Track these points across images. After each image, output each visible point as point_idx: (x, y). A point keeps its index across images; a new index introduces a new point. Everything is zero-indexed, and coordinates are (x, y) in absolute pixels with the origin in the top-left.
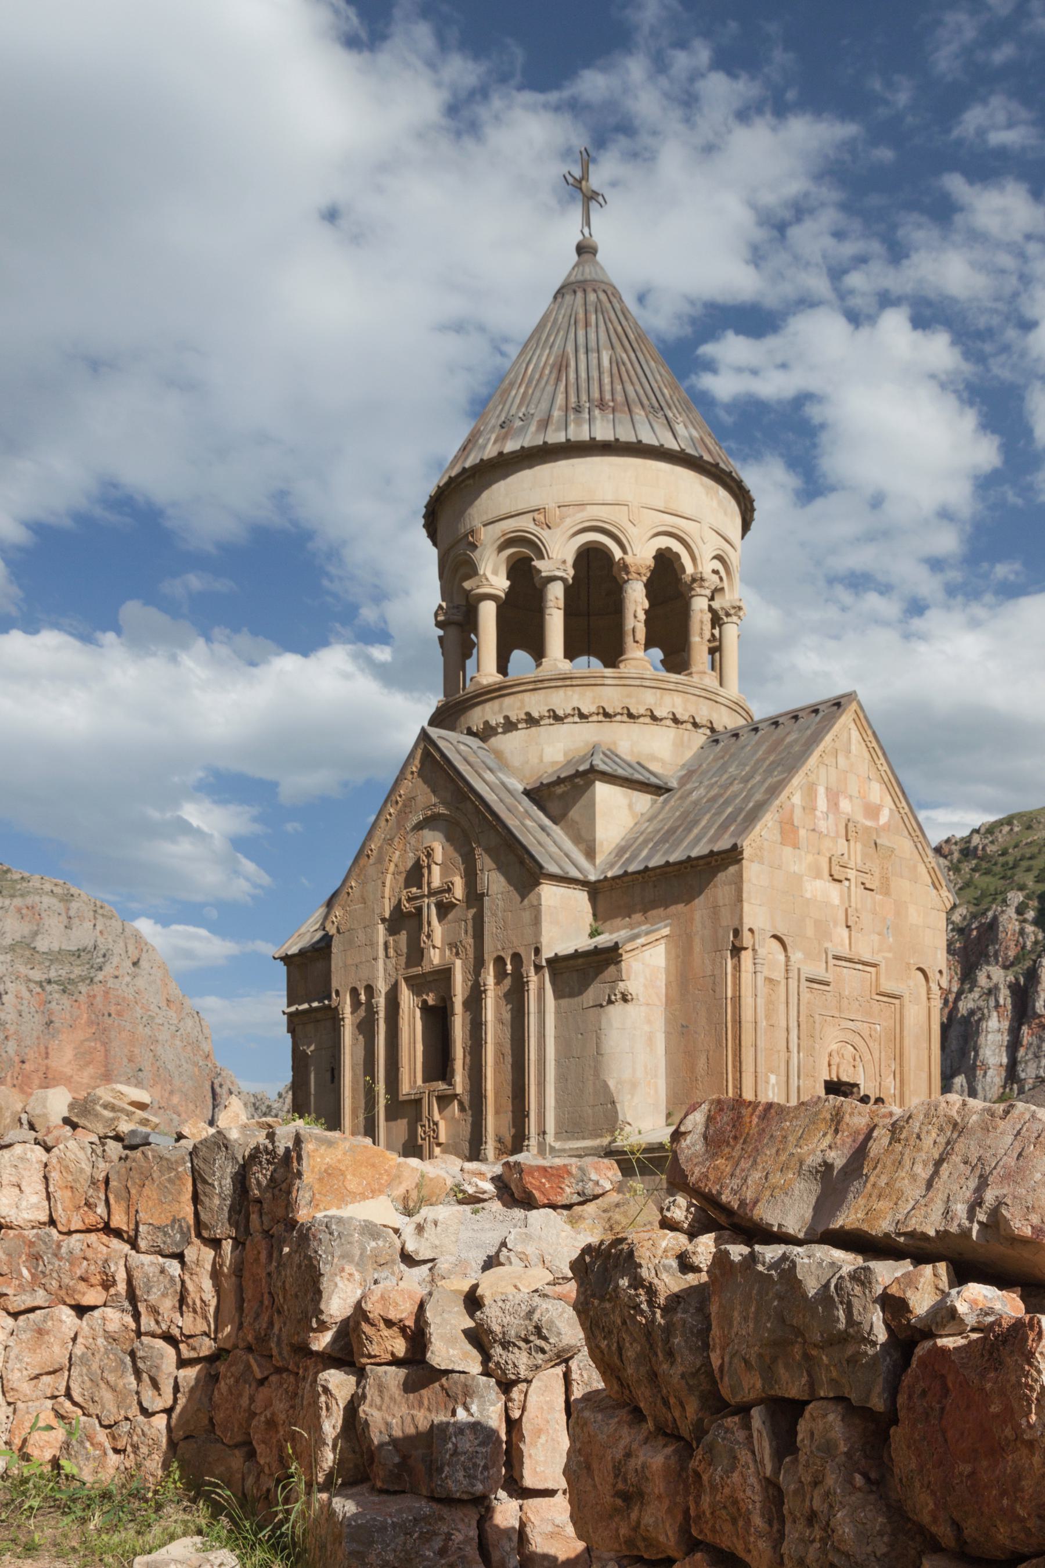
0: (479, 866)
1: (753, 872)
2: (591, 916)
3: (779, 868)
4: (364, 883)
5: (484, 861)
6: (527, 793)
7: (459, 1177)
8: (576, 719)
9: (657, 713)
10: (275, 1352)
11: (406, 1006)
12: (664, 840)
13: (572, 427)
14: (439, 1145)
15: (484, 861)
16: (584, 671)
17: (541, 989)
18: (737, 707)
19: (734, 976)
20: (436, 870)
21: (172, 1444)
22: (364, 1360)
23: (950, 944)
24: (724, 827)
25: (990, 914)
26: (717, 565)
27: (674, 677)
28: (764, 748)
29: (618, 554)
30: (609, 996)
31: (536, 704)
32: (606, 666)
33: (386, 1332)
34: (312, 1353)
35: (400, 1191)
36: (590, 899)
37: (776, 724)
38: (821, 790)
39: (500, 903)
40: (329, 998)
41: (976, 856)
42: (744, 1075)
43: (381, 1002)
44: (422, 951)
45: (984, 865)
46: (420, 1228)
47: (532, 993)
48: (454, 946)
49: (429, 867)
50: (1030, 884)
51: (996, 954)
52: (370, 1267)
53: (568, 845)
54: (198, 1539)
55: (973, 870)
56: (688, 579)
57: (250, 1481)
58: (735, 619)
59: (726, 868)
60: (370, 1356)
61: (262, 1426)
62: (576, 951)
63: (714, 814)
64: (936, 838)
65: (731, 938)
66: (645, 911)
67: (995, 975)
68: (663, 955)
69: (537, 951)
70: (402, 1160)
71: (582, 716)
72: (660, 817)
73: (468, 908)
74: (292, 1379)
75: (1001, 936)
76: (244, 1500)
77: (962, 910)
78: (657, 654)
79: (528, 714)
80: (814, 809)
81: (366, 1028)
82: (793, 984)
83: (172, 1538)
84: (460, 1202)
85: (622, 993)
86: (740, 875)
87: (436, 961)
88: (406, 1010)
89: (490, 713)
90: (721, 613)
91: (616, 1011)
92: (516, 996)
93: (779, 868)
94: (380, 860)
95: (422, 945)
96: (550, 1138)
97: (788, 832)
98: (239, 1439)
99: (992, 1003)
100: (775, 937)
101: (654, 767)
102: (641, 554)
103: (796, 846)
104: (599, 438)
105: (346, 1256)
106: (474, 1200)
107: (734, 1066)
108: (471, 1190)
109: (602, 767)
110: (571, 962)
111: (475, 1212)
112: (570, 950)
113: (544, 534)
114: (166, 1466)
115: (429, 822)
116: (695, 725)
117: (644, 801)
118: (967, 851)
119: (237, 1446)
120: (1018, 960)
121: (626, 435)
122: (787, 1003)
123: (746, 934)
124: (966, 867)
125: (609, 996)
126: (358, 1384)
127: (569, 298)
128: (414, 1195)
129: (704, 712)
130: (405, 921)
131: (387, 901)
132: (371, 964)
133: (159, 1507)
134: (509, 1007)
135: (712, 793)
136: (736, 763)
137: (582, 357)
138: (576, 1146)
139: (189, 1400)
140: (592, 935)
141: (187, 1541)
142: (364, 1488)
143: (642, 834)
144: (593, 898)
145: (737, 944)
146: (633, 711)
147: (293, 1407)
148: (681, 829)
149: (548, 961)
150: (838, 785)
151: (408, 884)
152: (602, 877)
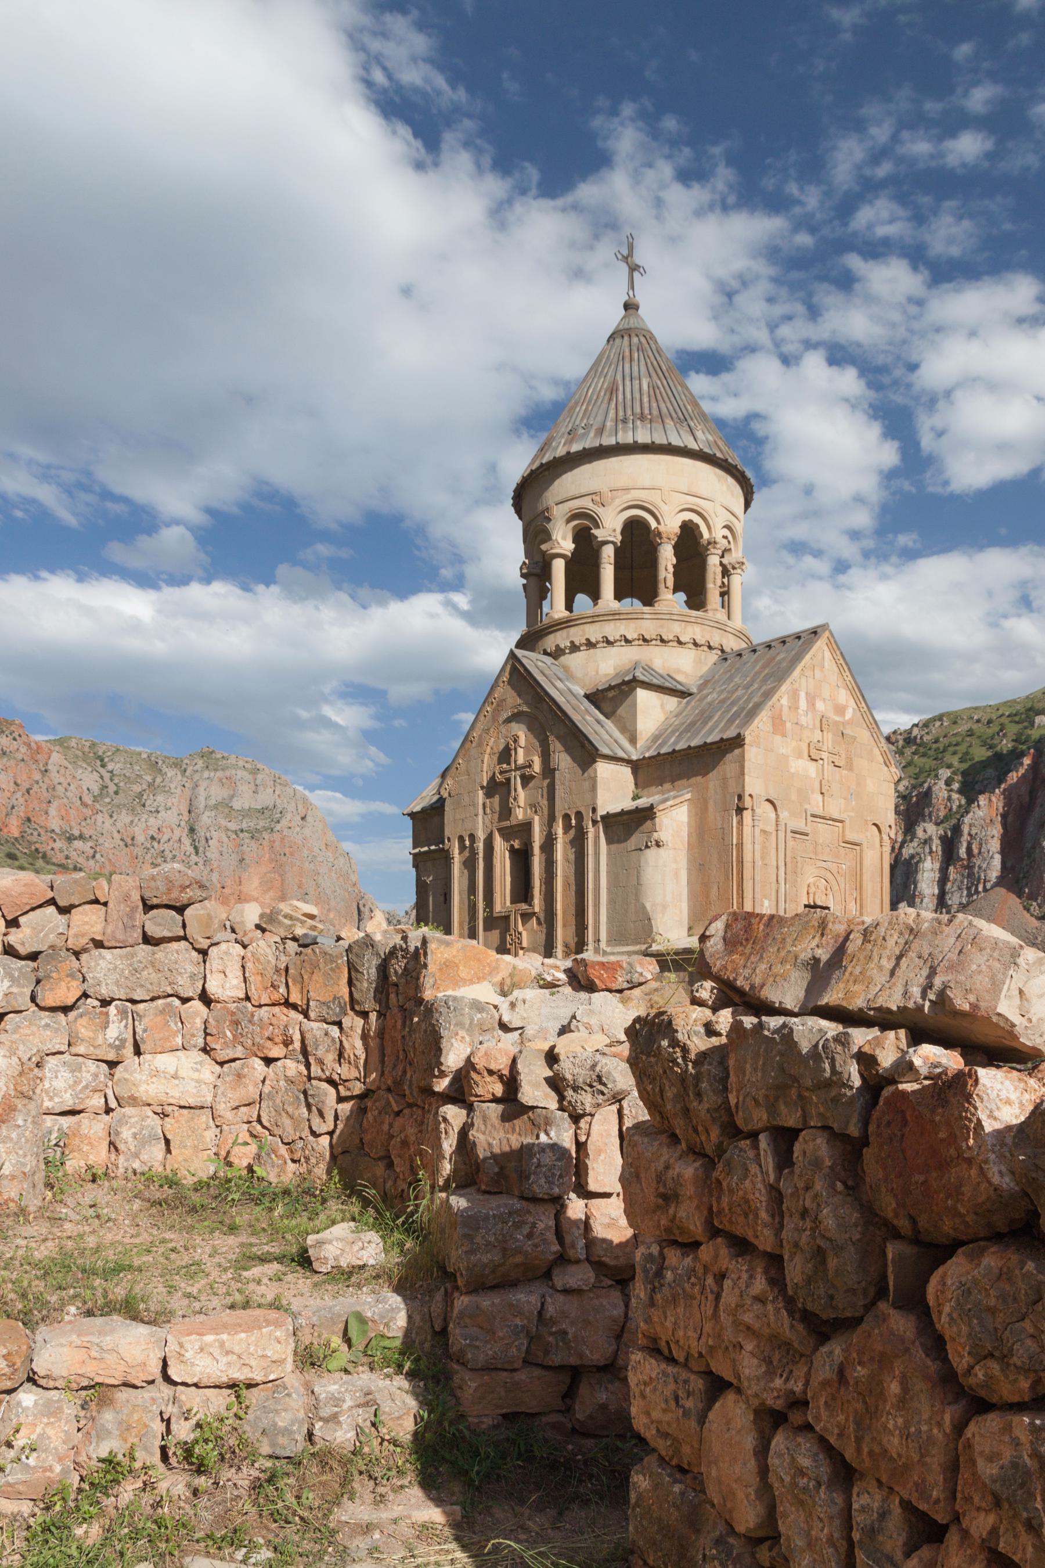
0: (552, 748)
1: (752, 753)
3: (772, 751)
4: (469, 761)
5: (556, 745)
6: (587, 696)
7: (541, 969)
9: (682, 639)
10: (407, 1092)
12: (687, 730)
13: (620, 434)
15: (556, 745)
16: (629, 609)
17: (597, 838)
18: (740, 635)
20: (520, 751)
21: (333, 1157)
22: (473, 1099)
23: (897, 806)
24: (731, 721)
25: (926, 785)
26: (726, 532)
27: (694, 613)
29: (653, 524)
31: (594, 632)
32: (645, 605)
33: (488, 1079)
34: (434, 1093)
35: (498, 978)
37: (769, 647)
38: (803, 695)
40: (443, 843)
41: (915, 743)
44: (510, 810)
45: (922, 750)
46: (513, 1005)
48: (534, 806)
50: (956, 763)
51: (930, 814)
52: (476, 1032)
53: (617, 734)
54: (352, 1224)
55: (914, 753)
56: (705, 543)
57: (389, 1183)
58: (739, 571)
60: (477, 1096)
61: (398, 1145)
64: (886, 730)
66: (673, 781)
67: (928, 830)
69: (594, 810)
70: (499, 956)
71: (627, 641)
73: (544, 778)
74: (420, 1112)
75: (934, 801)
76: (385, 1197)
77: (905, 783)
78: (682, 596)
79: (588, 640)
80: (797, 708)
81: (470, 864)
82: (781, 835)
83: (334, 1223)
84: (541, 987)
86: (742, 756)
87: (520, 817)
89: (559, 639)
90: (729, 567)
91: (651, 854)
92: (578, 842)
93: (772, 751)
94: (480, 745)
96: (603, 945)
97: (778, 725)
98: (382, 1153)
99: (927, 850)
100: (768, 800)
101: (680, 678)
102: (670, 525)
103: (784, 735)
104: (640, 441)
105: (460, 1024)
106: (551, 986)
108: (549, 978)
109: (642, 678)
111: (552, 994)
112: (619, 810)
113: (600, 510)
114: (329, 1172)
115: (516, 717)
116: (710, 647)
117: (672, 703)
118: (909, 740)
119: (380, 1159)
120: (946, 818)
121: (660, 439)
123: (747, 798)
124: (908, 752)
126: (468, 1115)
127: (618, 341)
128: (508, 982)
129: (716, 638)
130: (498, 788)
132: (473, 819)
133: (324, 1201)
135: (722, 696)
137: (628, 383)
139: (346, 1125)
140: (634, 799)
141: (345, 1225)
142: (471, 1190)
144: (635, 772)
146: (665, 638)
147: (420, 1131)
149: (602, 817)
150: (815, 689)
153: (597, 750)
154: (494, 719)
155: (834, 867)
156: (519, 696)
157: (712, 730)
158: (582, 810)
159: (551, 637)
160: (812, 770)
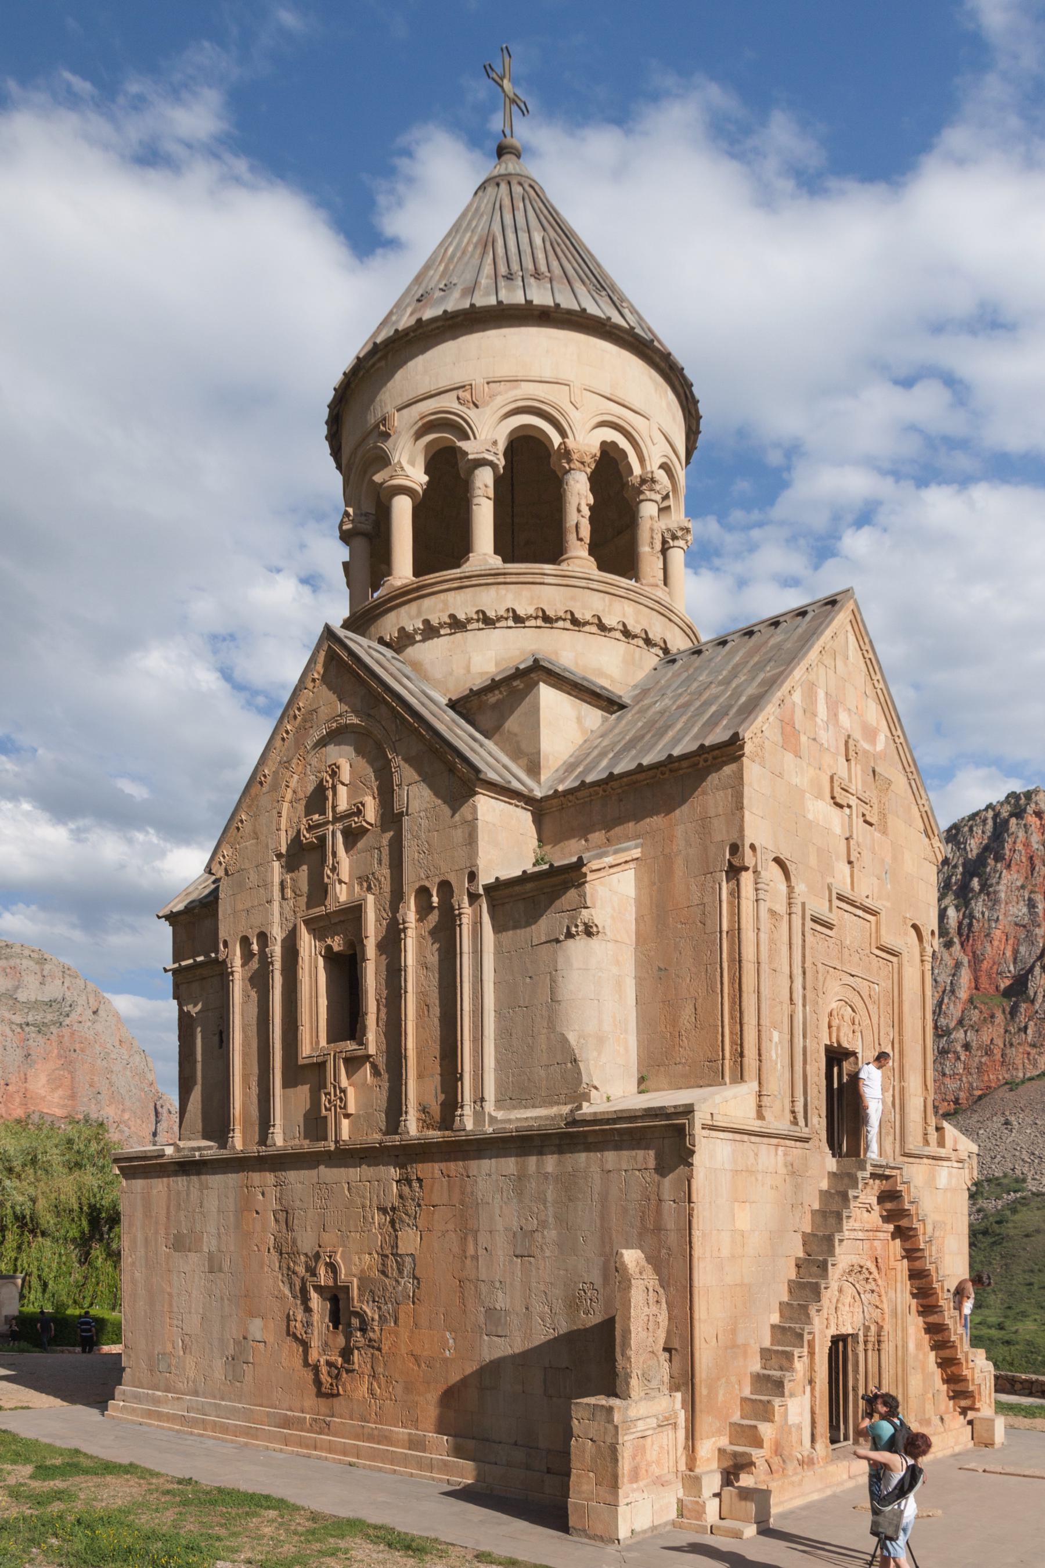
0: (396, 780)
2: (536, 843)
4: (255, 816)
5: (404, 773)
6: (453, 705)
8: (511, 623)
11: (307, 953)
14: (347, 1116)
15: (404, 773)
17: (477, 924)
19: (730, 903)
20: (342, 791)
28: (741, 653)
30: (568, 928)
36: (534, 821)
39: (424, 823)
42: (745, 1027)
43: (276, 950)
47: (465, 928)
48: (366, 880)
49: (334, 788)
59: (719, 769)
62: (524, 872)
63: (692, 717)
65: (728, 857)
68: (633, 882)
69: (472, 876)
72: (616, 731)
73: (384, 831)
82: (797, 920)
85: (585, 924)
87: (343, 898)
88: (307, 958)
91: (577, 947)
92: (445, 933)
94: (275, 787)
95: (326, 880)
96: (490, 1107)
100: (777, 860)
107: (732, 1017)
110: (517, 888)
115: (336, 735)
122: (790, 944)
125: (568, 928)
129: (658, 629)
131: (283, 834)
134: (437, 946)
135: (681, 701)
136: (707, 672)
138: (525, 1116)
143: (596, 747)
144: (538, 820)
145: (736, 862)
148: (649, 736)
149: (487, 888)
151: (308, 812)
152: (551, 792)
153: (477, 771)
154: (298, 743)
155: (863, 986)
156: (340, 700)
157: (676, 741)
158: (452, 878)
159: (391, 616)
160: (835, 821)
